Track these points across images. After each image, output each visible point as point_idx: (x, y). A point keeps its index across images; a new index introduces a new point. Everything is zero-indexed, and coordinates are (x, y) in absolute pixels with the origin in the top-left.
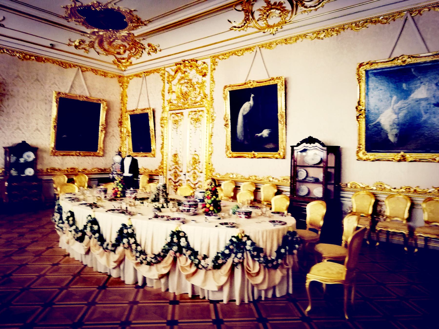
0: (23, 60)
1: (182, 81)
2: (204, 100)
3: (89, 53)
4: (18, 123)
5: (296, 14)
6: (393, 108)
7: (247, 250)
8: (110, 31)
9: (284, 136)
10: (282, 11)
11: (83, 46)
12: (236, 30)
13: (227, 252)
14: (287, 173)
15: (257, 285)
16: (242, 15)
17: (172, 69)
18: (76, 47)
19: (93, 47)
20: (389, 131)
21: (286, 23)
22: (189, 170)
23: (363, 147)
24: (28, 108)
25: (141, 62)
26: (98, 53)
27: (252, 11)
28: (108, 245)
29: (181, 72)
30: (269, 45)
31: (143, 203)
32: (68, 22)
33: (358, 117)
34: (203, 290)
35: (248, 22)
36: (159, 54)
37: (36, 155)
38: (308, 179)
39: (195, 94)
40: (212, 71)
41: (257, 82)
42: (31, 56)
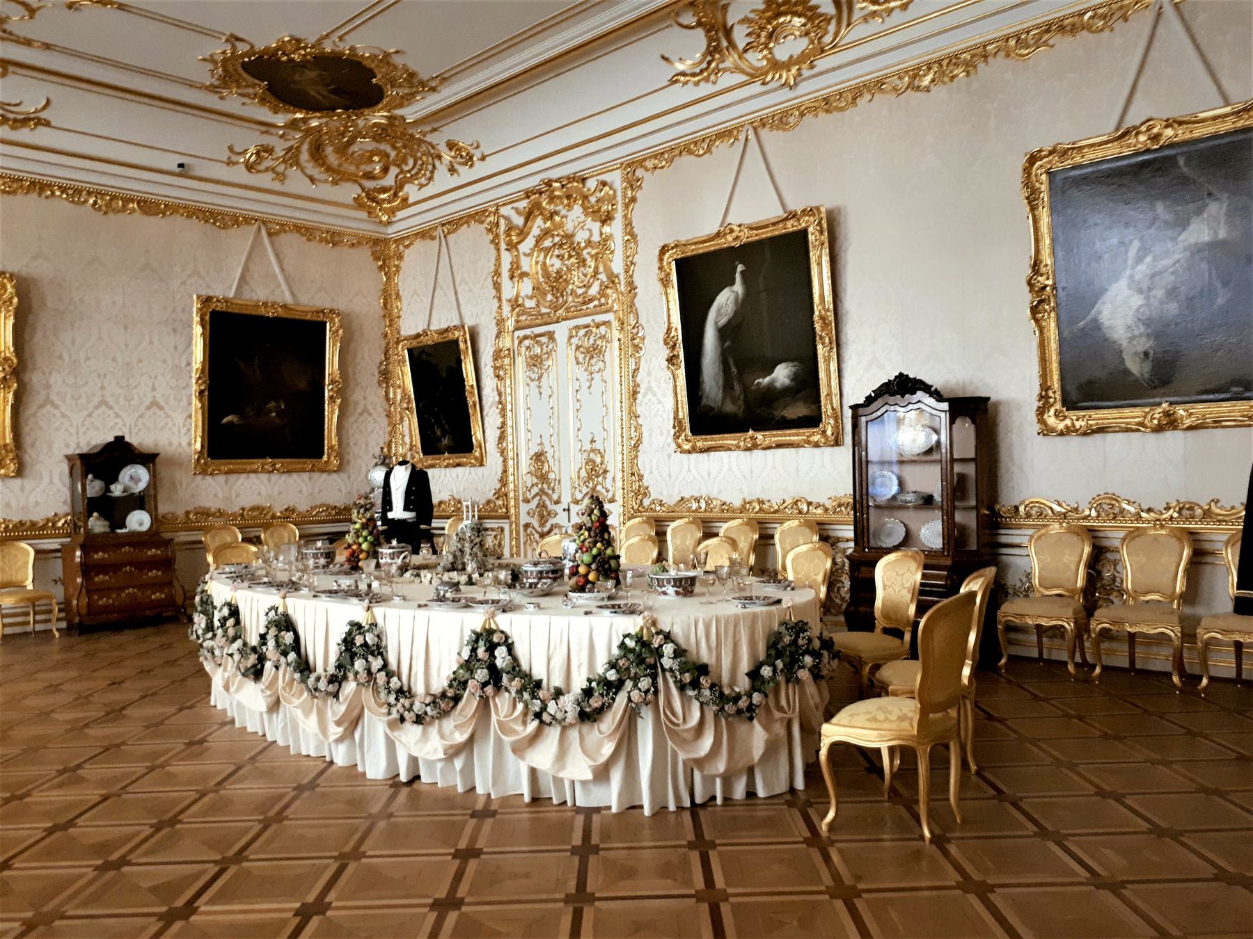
0: (105, 213)
1: (547, 243)
2: (609, 291)
3: (287, 182)
4: (103, 388)
5: (849, 25)
7: (664, 670)
8: (339, 115)
9: (834, 383)
10: (810, 19)
11: (267, 163)
12: (686, 83)
13: (612, 675)
14: (844, 487)
15: (700, 763)
16: (699, 39)
19: (298, 164)
21: (823, 51)
23: (1056, 394)
24: (127, 345)
25: (433, 195)
26: (312, 180)
27: (725, 25)
28: (318, 679)
30: (780, 120)
31: (418, 575)
32: (221, 98)
33: (1034, 310)
34: (558, 782)
35: (717, 56)
39: (585, 275)
40: (627, 206)
41: (751, 229)
42: (127, 200)
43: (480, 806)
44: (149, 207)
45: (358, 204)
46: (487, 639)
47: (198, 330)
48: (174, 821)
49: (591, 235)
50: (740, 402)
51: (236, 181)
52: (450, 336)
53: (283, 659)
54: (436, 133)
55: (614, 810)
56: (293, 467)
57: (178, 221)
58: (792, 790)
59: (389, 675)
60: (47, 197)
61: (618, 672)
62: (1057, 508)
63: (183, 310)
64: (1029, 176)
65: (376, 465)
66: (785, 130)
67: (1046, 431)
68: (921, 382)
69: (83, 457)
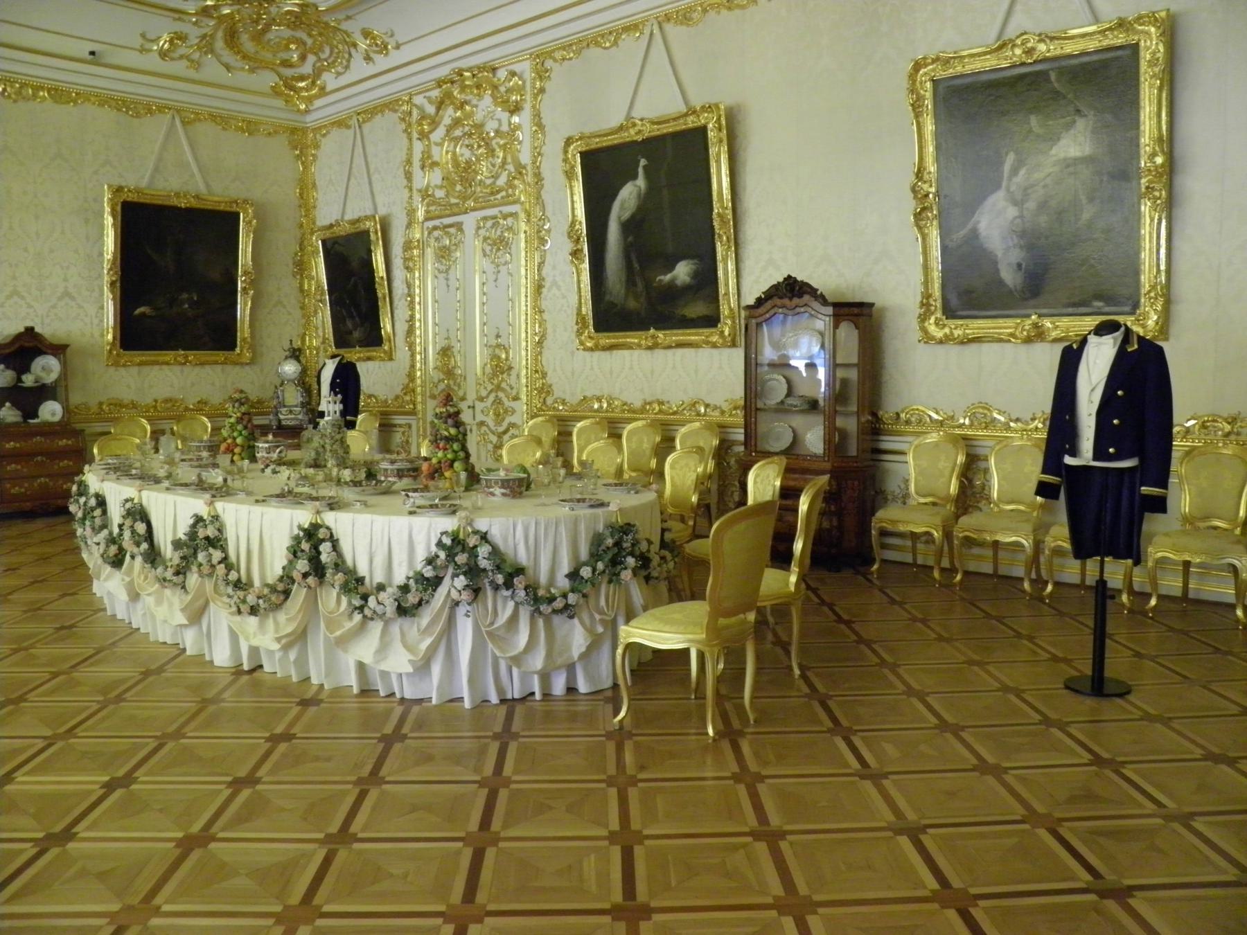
1: (458, 133)
2: (516, 182)
6: (1008, 190)
13: (429, 572)
14: (738, 392)
15: (516, 660)
17: (429, 98)
18: (163, 54)
20: (1000, 254)
22: (484, 393)
25: (350, 84)
26: (228, 68)
33: (918, 216)
34: (385, 675)
36: (396, 58)
37: (64, 365)
39: (493, 166)
40: (535, 96)
43: (309, 695)
45: (276, 92)
46: (312, 534)
47: (109, 220)
48: (22, 699)
49: (500, 125)
50: (642, 300)
51: (149, 68)
53: (136, 550)
54: (350, 22)
55: (434, 702)
56: (203, 359)
59: (229, 567)
61: (435, 568)
64: (914, 82)
65: (286, 358)
66: (688, 25)
67: (927, 338)
68: (807, 285)
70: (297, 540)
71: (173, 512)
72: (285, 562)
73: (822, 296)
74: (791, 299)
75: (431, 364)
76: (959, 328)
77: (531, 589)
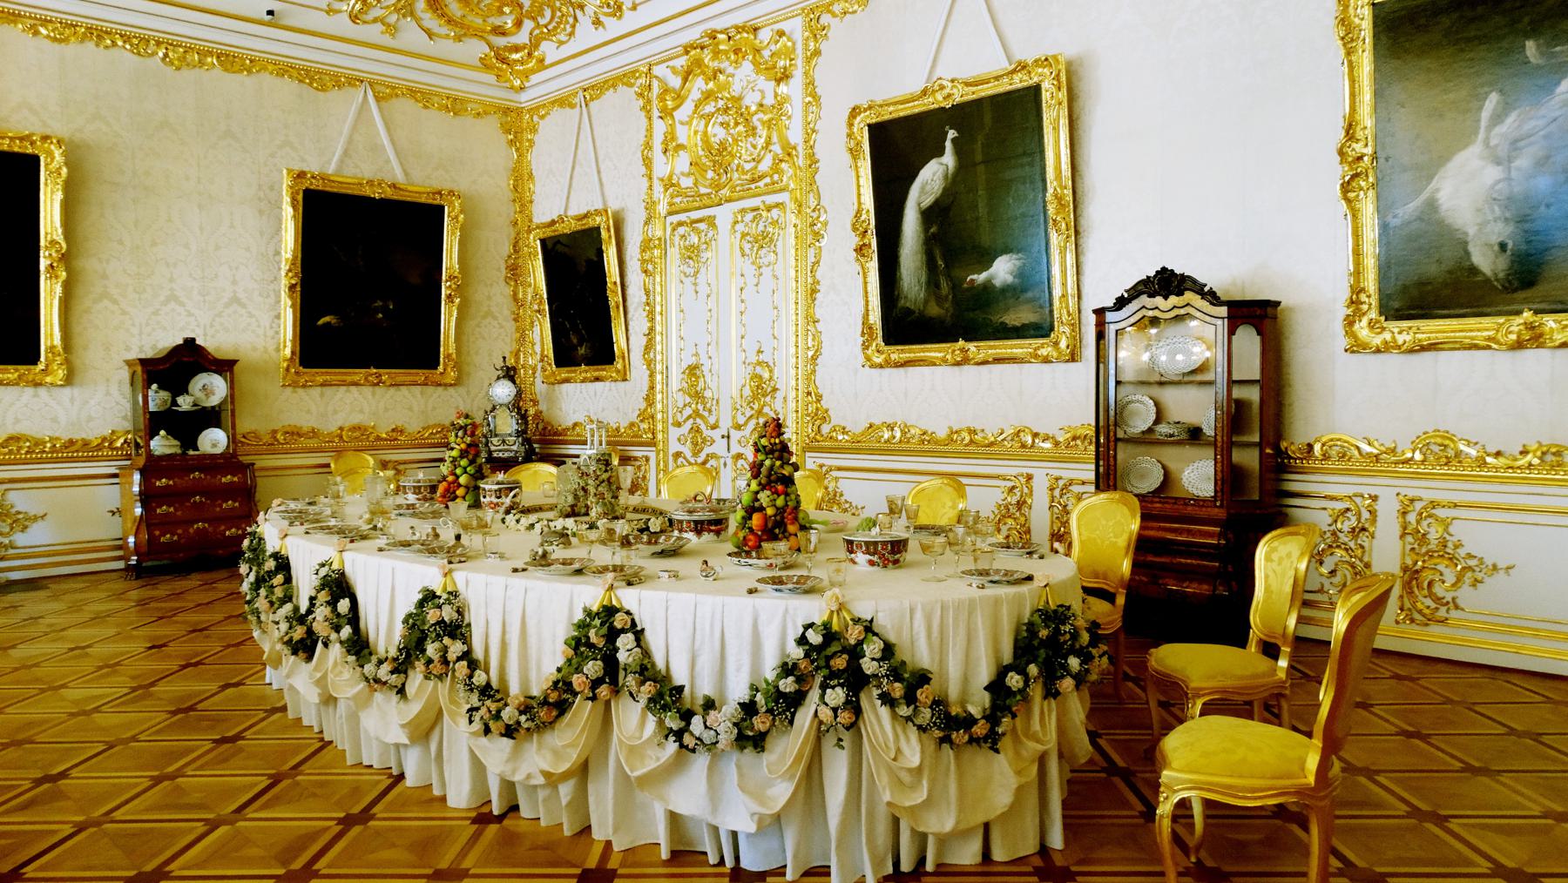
0: (178, 69)
1: (709, 108)
2: (783, 165)
4: (171, 280)
13: (788, 685)
14: (1084, 417)
17: (673, 69)
19: (412, 14)
20: (1472, 231)
22: (741, 420)
23: (1371, 299)
25: (573, 55)
26: (430, 35)
29: (703, 73)
33: (1346, 188)
36: (631, 20)
37: (232, 387)
38: (1163, 429)
39: (754, 147)
40: (808, 60)
41: (968, 84)
44: (229, 60)
47: (288, 212)
52: (590, 223)
53: (334, 636)
56: (400, 379)
57: (267, 79)
58: (1044, 850)
60: (107, 47)
62: (1366, 448)
63: (272, 188)
67: (1357, 347)
69: (144, 362)
70: (583, 626)
71: (389, 588)
72: (560, 662)
73: (1212, 293)
74: (1166, 298)
75: (675, 383)
76: (1404, 332)
77: (938, 703)
